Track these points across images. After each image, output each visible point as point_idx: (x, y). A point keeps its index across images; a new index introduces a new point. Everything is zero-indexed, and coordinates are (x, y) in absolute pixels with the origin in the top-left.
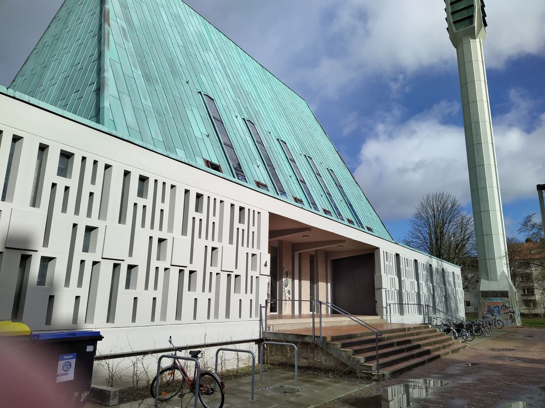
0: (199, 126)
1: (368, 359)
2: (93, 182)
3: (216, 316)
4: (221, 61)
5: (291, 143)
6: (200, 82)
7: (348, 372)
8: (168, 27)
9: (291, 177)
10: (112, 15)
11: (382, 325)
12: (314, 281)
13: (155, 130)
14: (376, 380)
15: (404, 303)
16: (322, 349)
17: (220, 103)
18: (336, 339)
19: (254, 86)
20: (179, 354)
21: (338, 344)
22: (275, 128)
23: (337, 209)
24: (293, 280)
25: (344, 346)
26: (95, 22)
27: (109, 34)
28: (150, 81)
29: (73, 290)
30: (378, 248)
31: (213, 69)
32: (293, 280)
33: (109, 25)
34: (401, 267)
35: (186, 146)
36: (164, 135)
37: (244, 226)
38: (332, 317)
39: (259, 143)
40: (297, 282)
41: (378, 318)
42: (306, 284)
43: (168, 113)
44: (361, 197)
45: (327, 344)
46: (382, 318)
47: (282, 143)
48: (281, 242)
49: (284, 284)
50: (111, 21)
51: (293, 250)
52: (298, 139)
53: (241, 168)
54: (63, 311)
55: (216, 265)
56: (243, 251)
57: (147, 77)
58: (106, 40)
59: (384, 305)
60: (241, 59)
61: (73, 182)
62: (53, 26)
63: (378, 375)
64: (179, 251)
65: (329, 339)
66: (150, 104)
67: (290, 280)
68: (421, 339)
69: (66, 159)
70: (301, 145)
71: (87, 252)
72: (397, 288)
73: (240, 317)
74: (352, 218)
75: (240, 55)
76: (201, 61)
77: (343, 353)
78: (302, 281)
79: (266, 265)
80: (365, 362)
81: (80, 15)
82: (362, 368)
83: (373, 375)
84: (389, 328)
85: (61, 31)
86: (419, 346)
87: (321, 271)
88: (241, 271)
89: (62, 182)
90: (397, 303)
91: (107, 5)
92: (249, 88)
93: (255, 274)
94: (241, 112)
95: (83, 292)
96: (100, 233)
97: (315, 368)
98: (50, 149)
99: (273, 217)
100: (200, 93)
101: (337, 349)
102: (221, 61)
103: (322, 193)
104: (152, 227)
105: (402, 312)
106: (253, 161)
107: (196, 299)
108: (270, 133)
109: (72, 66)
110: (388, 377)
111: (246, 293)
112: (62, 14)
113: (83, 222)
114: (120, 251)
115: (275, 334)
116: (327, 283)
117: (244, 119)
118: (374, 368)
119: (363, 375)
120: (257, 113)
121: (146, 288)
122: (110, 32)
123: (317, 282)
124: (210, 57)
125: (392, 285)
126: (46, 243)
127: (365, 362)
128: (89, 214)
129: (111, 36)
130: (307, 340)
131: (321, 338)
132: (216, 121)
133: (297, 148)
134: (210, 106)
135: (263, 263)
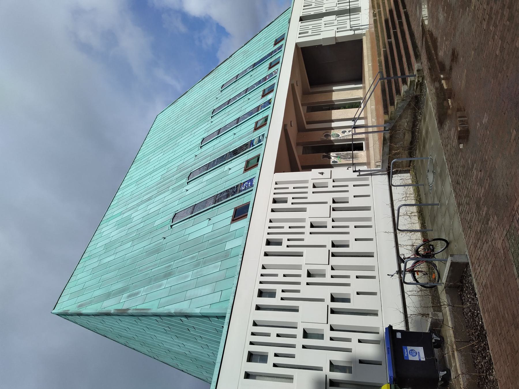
0: (201, 228)
1: (404, 82)
2: (268, 335)
3: (368, 219)
4: (138, 205)
5: (201, 132)
6: (162, 226)
7: (416, 102)
8: (118, 255)
9: (235, 134)
10: (120, 307)
11: (371, 34)
12: (333, 106)
13: (213, 269)
14: (423, 79)
15: (348, 8)
16: (397, 122)
17: (179, 208)
18: (386, 112)
19: (154, 171)
20: (403, 269)
21: (391, 109)
22: (191, 150)
23: (260, 82)
24: (332, 129)
25: (392, 104)
26: (127, 319)
27: (136, 309)
28: (170, 273)
29: (354, 345)
30: (296, 44)
31: (146, 213)
32: (332, 129)
33: (128, 309)
34: (312, 13)
35: (221, 240)
36: (215, 260)
37: (290, 197)
38: (365, 83)
39: (209, 167)
40: (334, 125)
41: (364, 38)
42: (336, 114)
43: (196, 256)
44: (245, 52)
45: (391, 119)
46: (364, 34)
47: (204, 142)
48: (298, 144)
49: (336, 138)
50: (125, 307)
51: (308, 147)
52: (196, 125)
53: (234, 187)
54: (370, 351)
55: (326, 222)
56: (312, 197)
57: (168, 275)
58: (142, 311)
59: (351, 33)
60: (131, 184)
61: (271, 351)
62: (134, 347)
63: (418, 77)
64: (316, 258)
65: (387, 117)
66: (191, 273)
67: (333, 132)
68: (385, 9)
69: (253, 356)
70: (202, 121)
71: (323, 335)
72: (334, 17)
73: (369, 196)
74: (267, 64)
75: (128, 186)
76: (142, 225)
77: (399, 106)
78: (333, 119)
79: (322, 173)
80: (407, 84)
81: (121, 329)
82: (412, 89)
83: (418, 81)
84: (373, 26)
85: (137, 341)
86: (391, 11)
87: (320, 98)
88: (328, 198)
89: (272, 359)
90: (348, 17)
91: (111, 311)
92: (157, 177)
93: (331, 184)
94: (182, 186)
95: (355, 337)
96: (308, 326)
97: (413, 127)
98: (248, 370)
99: (278, 169)
100: (171, 226)
101: (396, 110)
102: (138, 205)
103: (246, 98)
104: (298, 283)
105: (357, 10)
106: (225, 174)
107: (356, 240)
108: (196, 156)
109: (166, 333)
110: (419, 64)
111: (347, 191)
112: (121, 340)
113: (300, 341)
114: (321, 309)
115: (383, 162)
116: (333, 91)
117: (188, 183)
118: (412, 78)
119: (418, 89)
120: (180, 169)
121: (348, 285)
122: (135, 308)
123: (332, 101)
124: (137, 216)
125: (331, 24)
126: (320, 369)
127: (407, 84)
128: (294, 336)
129: (138, 307)
130: (388, 136)
131: (385, 125)
132: (195, 210)
133: (205, 126)
134: (182, 217)
135: (321, 176)
